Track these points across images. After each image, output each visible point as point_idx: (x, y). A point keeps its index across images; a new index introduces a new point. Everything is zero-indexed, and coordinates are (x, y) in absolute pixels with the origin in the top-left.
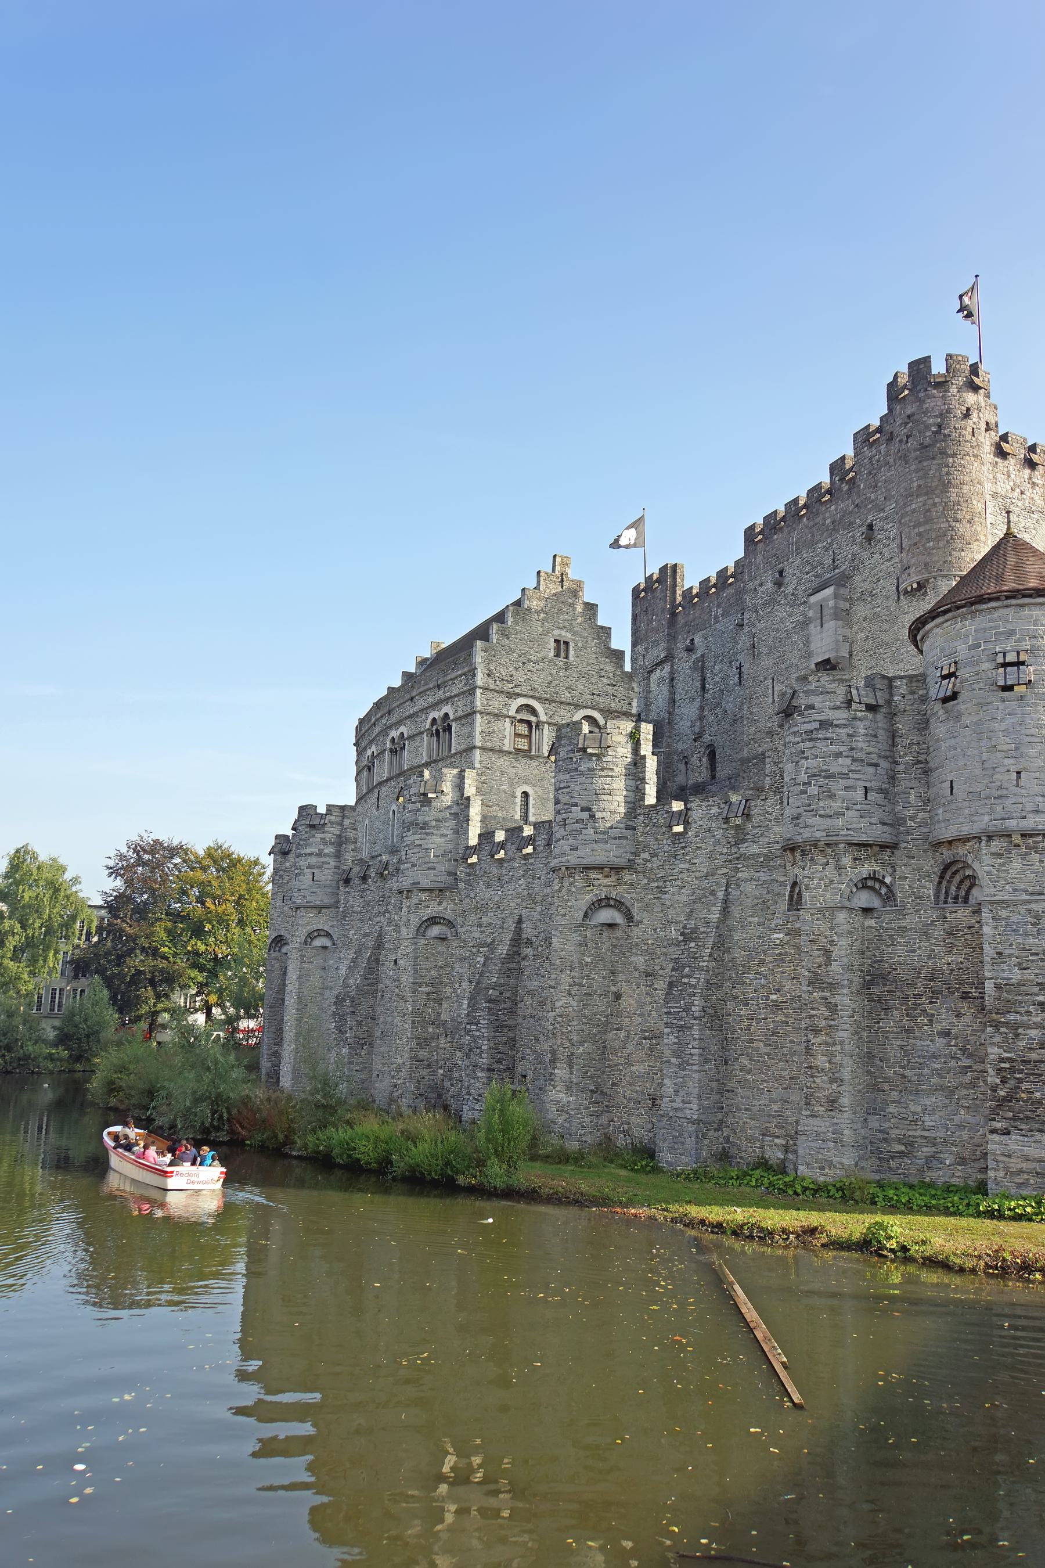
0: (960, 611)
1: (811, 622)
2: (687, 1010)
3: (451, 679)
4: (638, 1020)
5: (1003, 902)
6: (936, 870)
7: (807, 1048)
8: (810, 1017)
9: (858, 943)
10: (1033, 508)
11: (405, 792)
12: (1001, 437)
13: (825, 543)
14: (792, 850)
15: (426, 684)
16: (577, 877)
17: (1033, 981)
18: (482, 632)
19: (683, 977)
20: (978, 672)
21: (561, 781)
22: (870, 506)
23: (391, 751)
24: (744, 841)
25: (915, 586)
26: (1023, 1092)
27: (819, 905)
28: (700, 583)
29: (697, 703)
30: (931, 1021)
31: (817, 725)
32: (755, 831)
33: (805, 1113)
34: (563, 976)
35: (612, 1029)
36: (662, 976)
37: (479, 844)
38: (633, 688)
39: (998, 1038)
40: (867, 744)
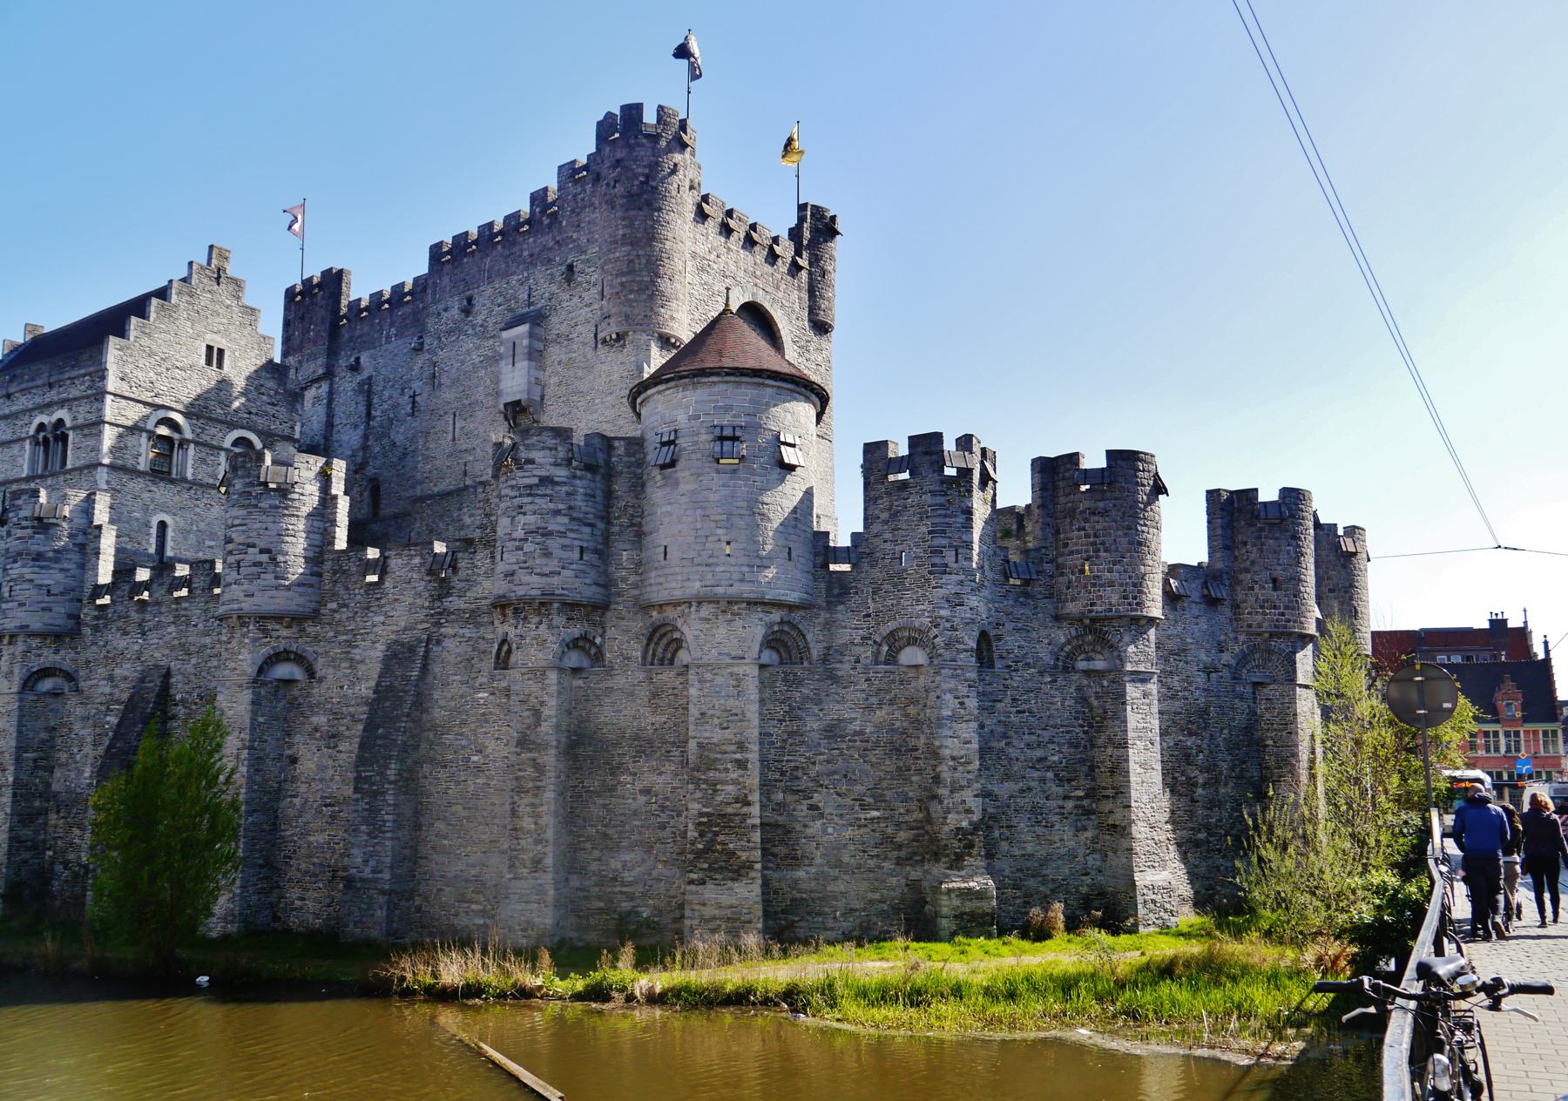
1: (501, 359)
2: (381, 774)
3: (70, 378)
6: (644, 632)
8: (517, 779)
10: (727, 273)
11: (11, 515)
12: (703, 197)
14: (503, 607)
15: (33, 379)
16: (251, 627)
18: (114, 321)
19: (377, 738)
20: (696, 442)
21: (236, 518)
22: (571, 246)
24: (449, 594)
25: (614, 336)
26: (719, 844)
27: (530, 665)
28: (371, 296)
29: (360, 431)
31: (536, 481)
32: (463, 584)
33: (508, 876)
35: (285, 797)
37: (113, 583)
39: (698, 795)
40: (585, 504)
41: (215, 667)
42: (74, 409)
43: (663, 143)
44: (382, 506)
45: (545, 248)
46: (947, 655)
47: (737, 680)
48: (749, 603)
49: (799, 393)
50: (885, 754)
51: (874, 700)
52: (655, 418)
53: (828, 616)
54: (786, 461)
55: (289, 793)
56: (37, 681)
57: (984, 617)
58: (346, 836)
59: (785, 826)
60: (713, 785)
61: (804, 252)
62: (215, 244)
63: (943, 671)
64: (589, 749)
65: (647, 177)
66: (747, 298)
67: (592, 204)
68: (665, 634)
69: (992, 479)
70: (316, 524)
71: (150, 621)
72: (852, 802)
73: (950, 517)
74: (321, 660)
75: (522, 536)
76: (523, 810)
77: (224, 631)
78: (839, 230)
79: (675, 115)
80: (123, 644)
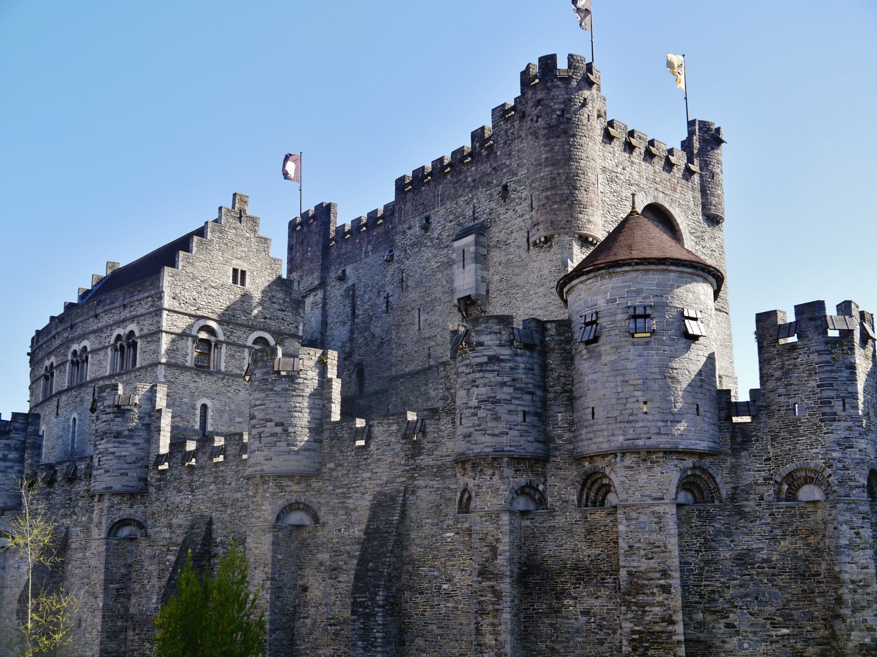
0: (601, 272)
2: (372, 599)
3: (138, 300)
4: (323, 609)
5: (633, 505)
6: (578, 479)
7: (477, 629)
8: (480, 603)
9: (517, 540)
10: (632, 182)
11: (99, 404)
13: (467, 198)
14: (464, 462)
15: (112, 303)
16: (271, 484)
17: (656, 568)
19: (368, 570)
20: (614, 322)
21: (257, 399)
22: (505, 170)
23: (72, 362)
24: (420, 454)
25: (543, 239)
27: (487, 509)
28: (352, 222)
30: (576, 603)
31: (485, 359)
32: (430, 445)
34: (257, 572)
35: (300, 618)
36: (346, 570)
37: (170, 453)
38: (300, 314)
39: (630, 615)
40: (525, 376)
41: (244, 516)
42: (141, 323)
43: (574, 83)
44: (366, 385)
45: (485, 174)
46: (841, 491)
47: (658, 517)
48: (665, 453)
49: (698, 275)
50: (791, 579)
51: (778, 532)
52: (579, 303)
53: (734, 460)
54: (690, 332)
55: (302, 615)
56: (118, 529)
57: (873, 457)
58: (347, 650)
59: (706, 642)
60: (642, 606)
61: (695, 160)
62: (238, 192)
63: (838, 505)
64: (536, 577)
65: (563, 111)
66: (650, 200)
67: (520, 137)
68: (596, 480)
69: (871, 338)
70: (317, 401)
71: (197, 481)
72: (764, 621)
73: (835, 372)
74: (323, 509)
75: (476, 404)
76: (486, 629)
77: (251, 488)
78: (724, 138)
79: (583, 60)
80: (178, 499)
